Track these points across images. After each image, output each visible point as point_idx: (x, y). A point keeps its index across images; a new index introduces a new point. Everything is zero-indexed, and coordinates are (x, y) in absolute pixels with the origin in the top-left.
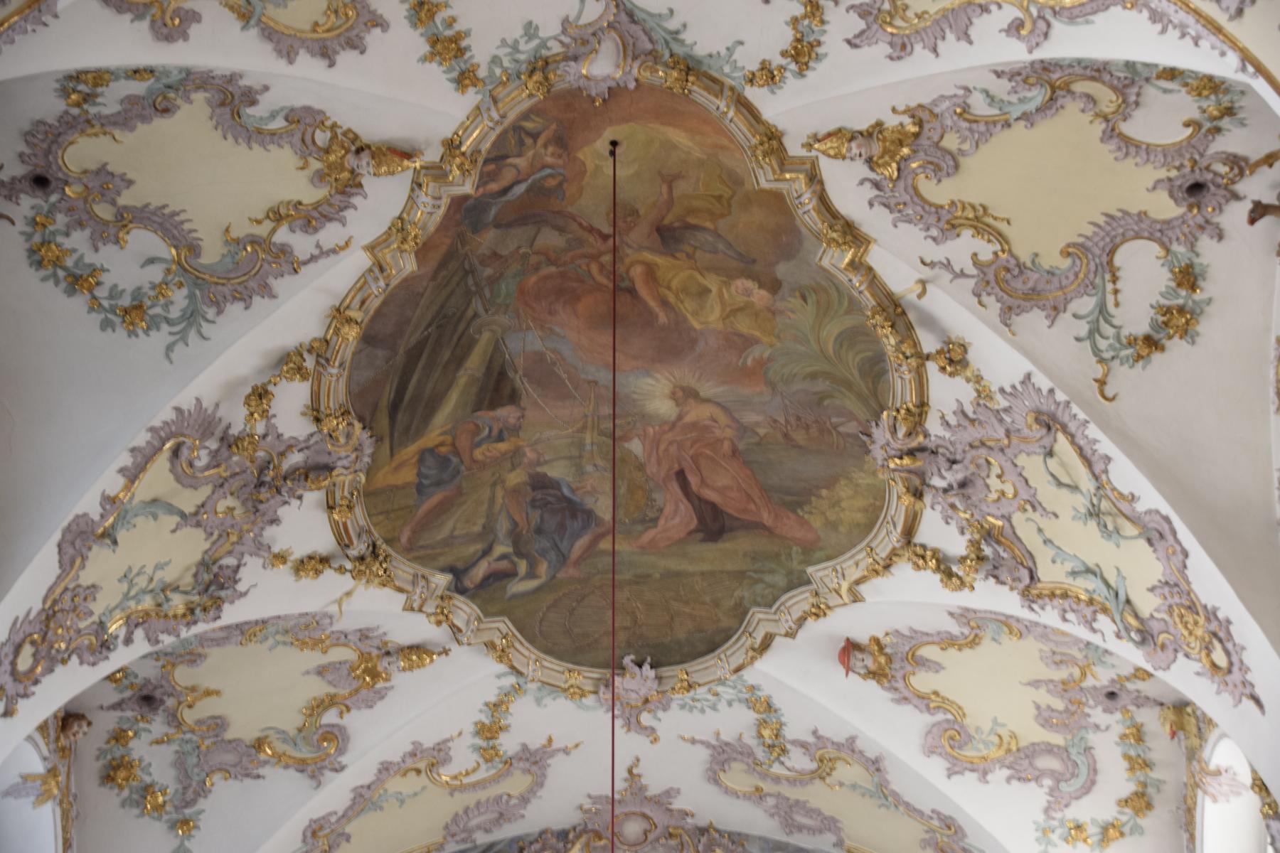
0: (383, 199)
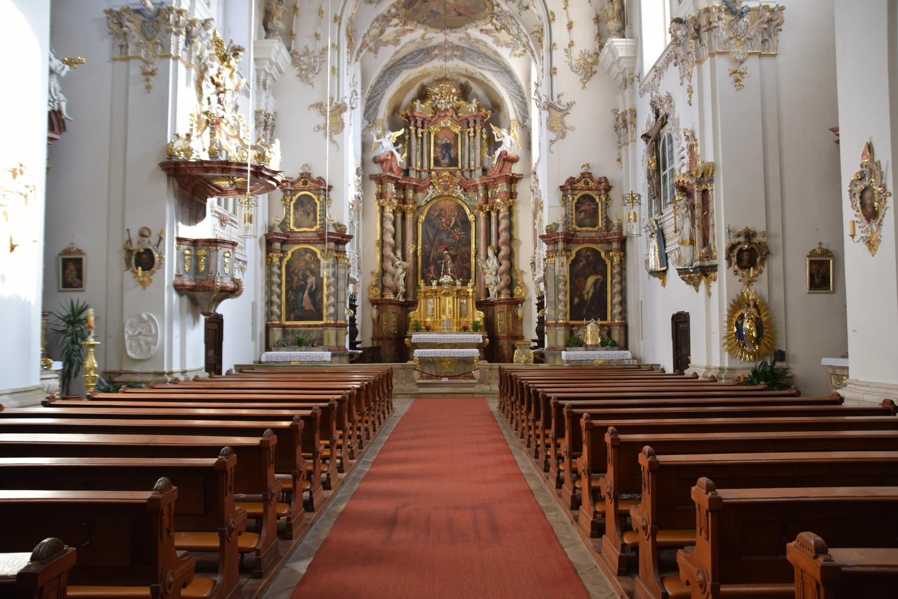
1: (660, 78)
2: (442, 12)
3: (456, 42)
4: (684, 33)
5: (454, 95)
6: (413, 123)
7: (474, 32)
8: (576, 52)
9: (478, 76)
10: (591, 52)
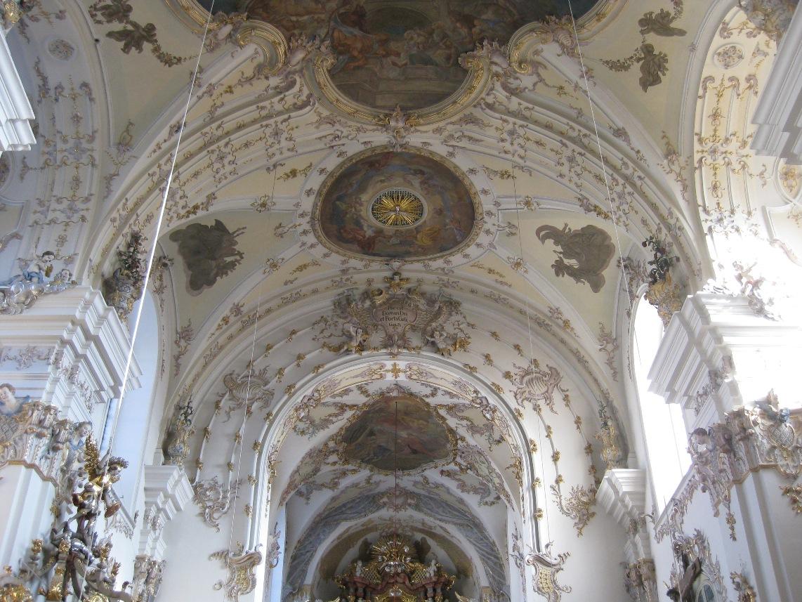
0: (349, 414)
1: (683, 513)
2: (393, 449)
3: (410, 487)
4: (710, 447)
5: (407, 555)
6: (352, 590)
7: (433, 474)
8: (566, 490)
9: (438, 531)
10: (586, 489)
